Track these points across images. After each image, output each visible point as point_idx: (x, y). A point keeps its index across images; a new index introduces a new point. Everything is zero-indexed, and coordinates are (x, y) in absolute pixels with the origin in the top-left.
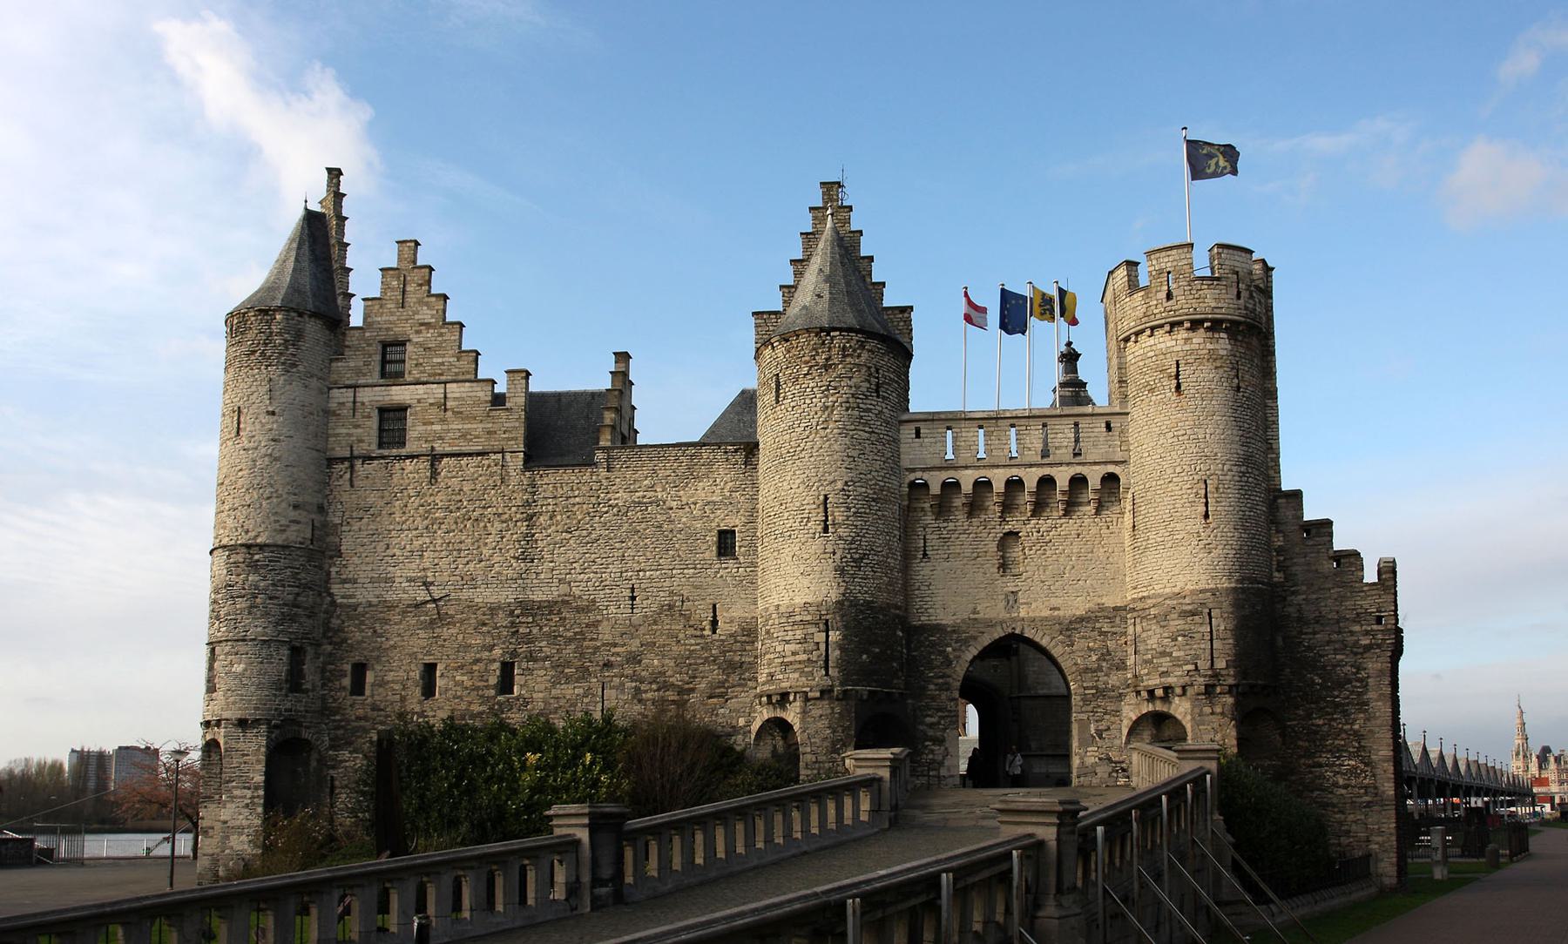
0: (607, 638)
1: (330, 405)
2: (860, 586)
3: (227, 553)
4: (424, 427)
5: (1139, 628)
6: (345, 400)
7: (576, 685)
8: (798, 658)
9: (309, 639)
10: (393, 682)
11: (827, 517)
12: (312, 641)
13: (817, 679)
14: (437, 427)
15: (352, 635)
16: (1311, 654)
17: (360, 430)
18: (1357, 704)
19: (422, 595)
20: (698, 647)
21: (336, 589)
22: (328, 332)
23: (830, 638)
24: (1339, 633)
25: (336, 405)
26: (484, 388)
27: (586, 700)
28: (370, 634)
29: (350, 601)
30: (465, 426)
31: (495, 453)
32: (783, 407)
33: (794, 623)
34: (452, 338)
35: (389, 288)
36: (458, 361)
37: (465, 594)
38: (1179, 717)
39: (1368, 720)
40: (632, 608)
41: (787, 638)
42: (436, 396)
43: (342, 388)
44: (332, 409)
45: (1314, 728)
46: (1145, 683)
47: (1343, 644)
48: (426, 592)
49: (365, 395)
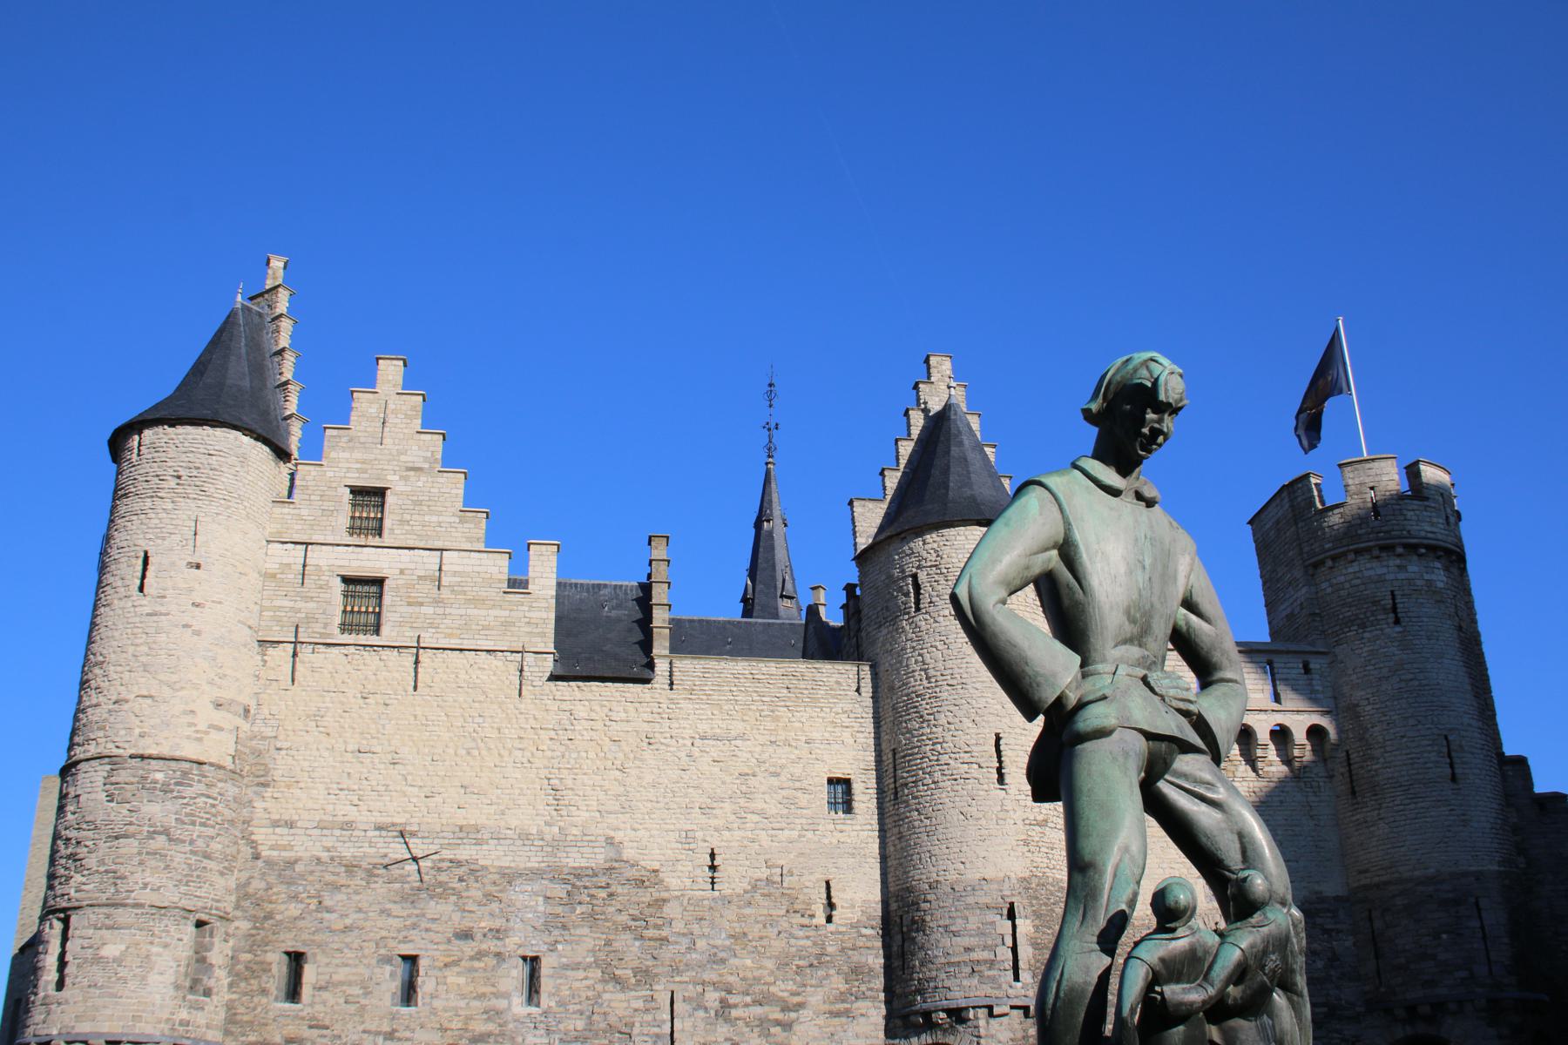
0: (679, 926)
1: (267, 566)
2: (1048, 858)
3: (108, 767)
4: (411, 609)
5: (1378, 924)
6: (291, 560)
7: (633, 993)
8: (975, 956)
9: (217, 909)
10: (350, 984)
11: (1000, 761)
12: (222, 914)
13: (1005, 986)
14: (424, 609)
15: (283, 907)
17: (312, 605)
19: (398, 851)
20: (809, 943)
21: (261, 835)
22: (273, 464)
23: (1018, 930)
25: (277, 566)
26: (498, 562)
27: (649, 1017)
28: (312, 907)
29: (284, 854)
30: (469, 611)
31: (512, 652)
32: (927, 617)
33: (968, 907)
34: (454, 491)
35: (363, 416)
36: (461, 522)
37: (464, 853)
40: (713, 883)
41: (953, 928)
42: (427, 566)
43: (286, 543)
44: (268, 571)
48: (405, 846)
49: (317, 556)
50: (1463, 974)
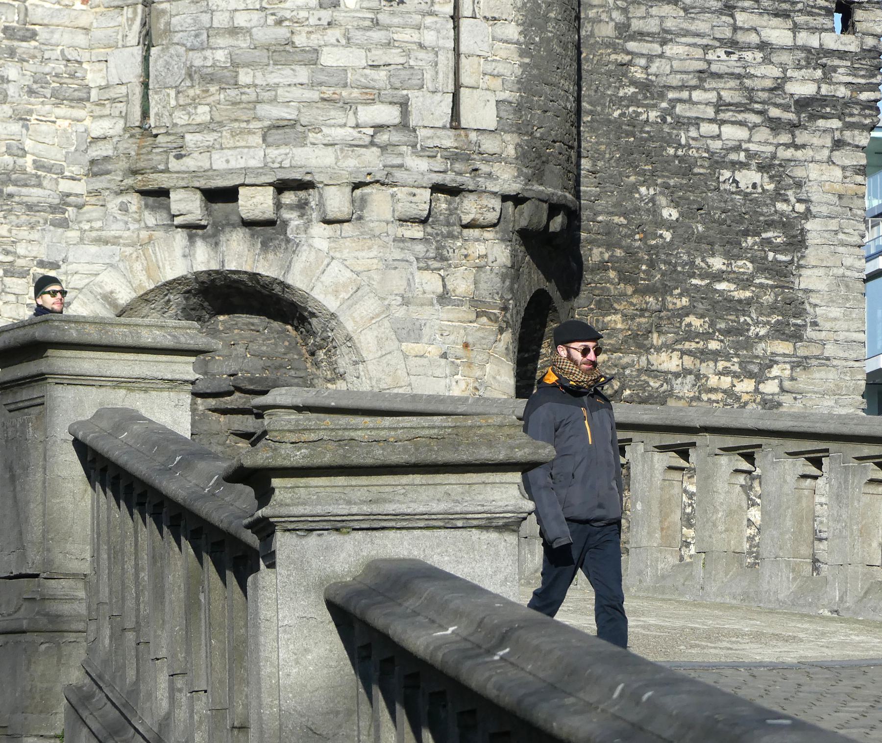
16: (653, 115)
18: (773, 309)
24: (732, 45)
38: (331, 304)
39: (801, 364)
45: (654, 384)
46: (189, 163)
47: (743, 87)
50: (389, 114)
